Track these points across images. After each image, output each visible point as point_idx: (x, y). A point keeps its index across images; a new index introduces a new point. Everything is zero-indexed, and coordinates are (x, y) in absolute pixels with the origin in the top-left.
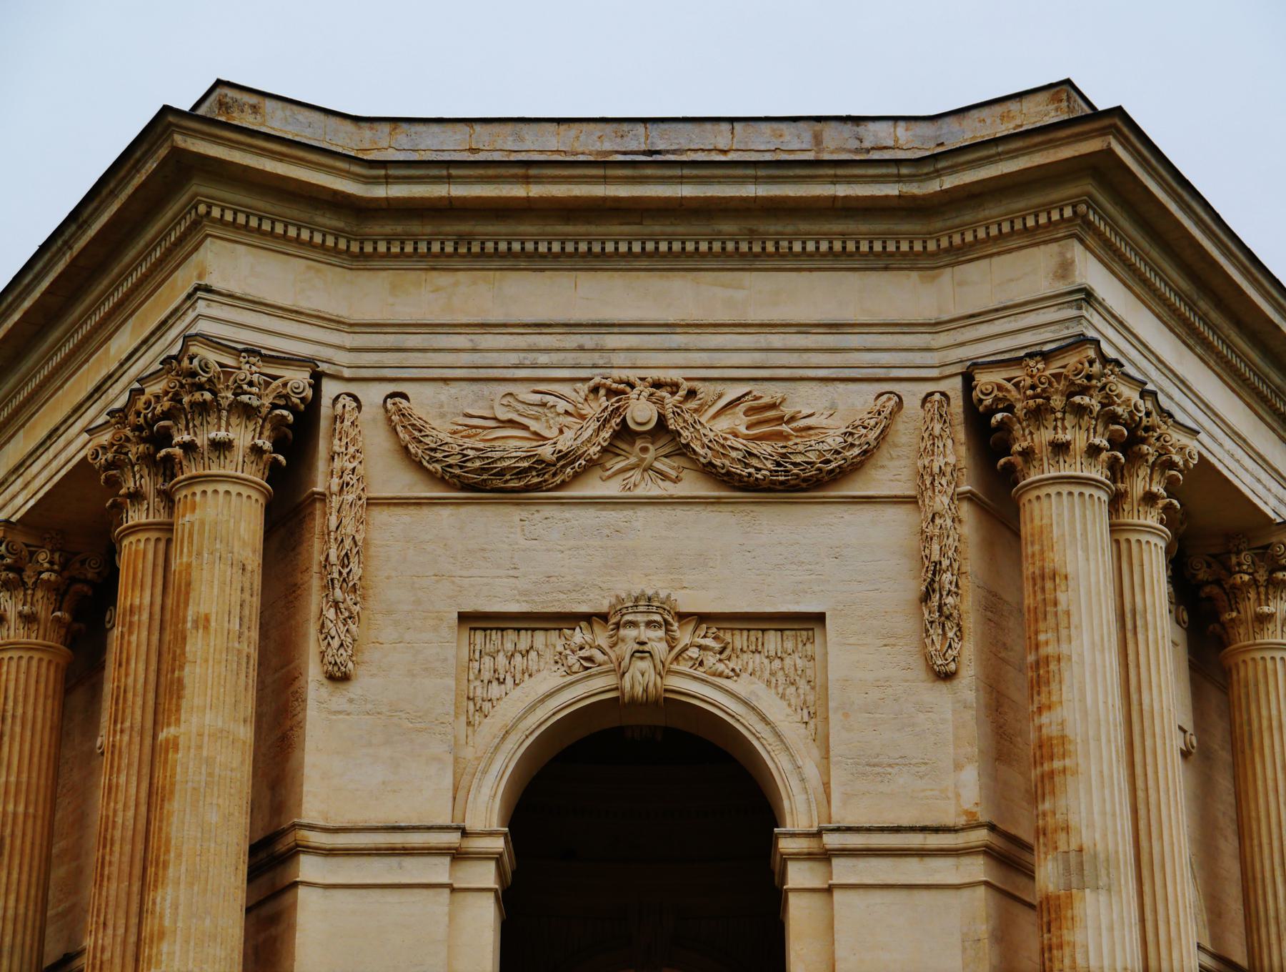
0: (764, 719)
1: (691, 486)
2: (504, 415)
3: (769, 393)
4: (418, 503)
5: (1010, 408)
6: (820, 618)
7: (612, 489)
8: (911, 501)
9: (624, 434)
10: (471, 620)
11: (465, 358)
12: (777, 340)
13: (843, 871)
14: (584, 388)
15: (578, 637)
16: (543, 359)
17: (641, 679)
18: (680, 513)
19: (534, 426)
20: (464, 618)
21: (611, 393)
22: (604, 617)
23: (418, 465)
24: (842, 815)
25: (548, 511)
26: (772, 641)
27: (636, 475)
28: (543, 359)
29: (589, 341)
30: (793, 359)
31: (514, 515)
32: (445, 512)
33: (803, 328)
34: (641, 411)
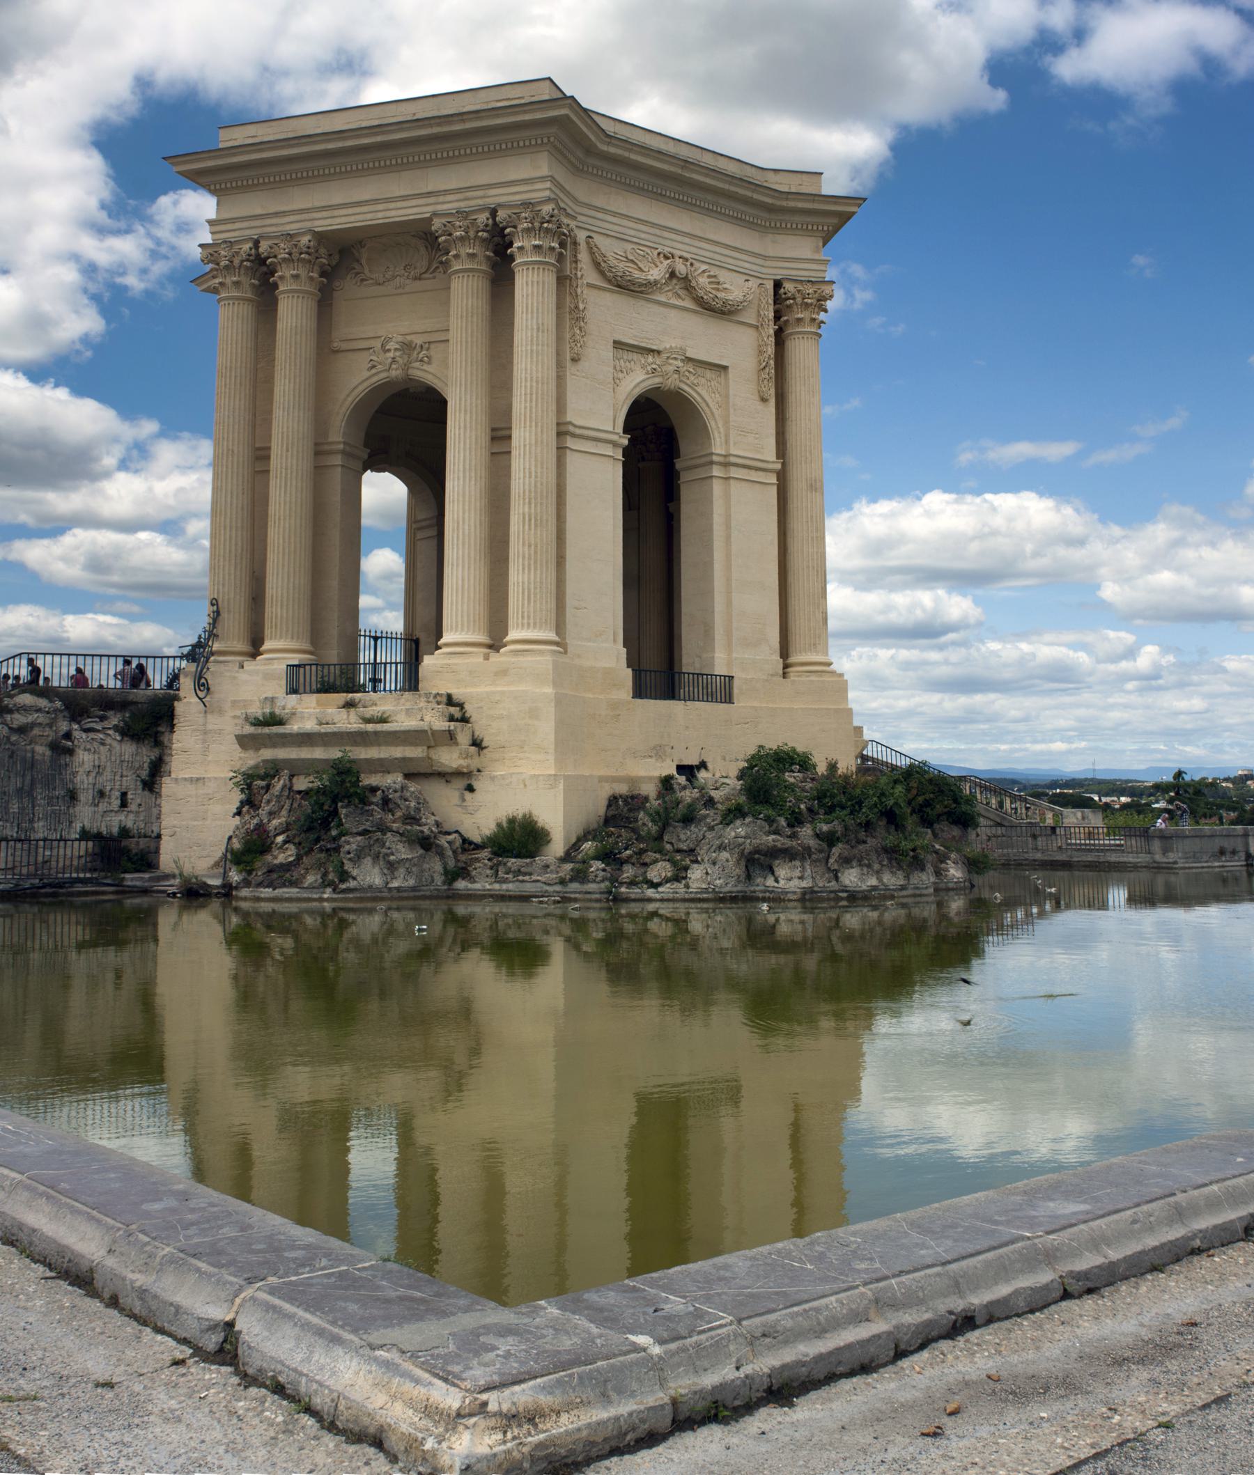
0: (708, 405)
1: (688, 304)
2: (631, 257)
3: (714, 271)
4: (605, 289)
5: (794, 299)
6: (725, 368)
7: (662, 298)
8: (757, 327)
9: (673, 275)
10: (618, 345)
11: (616, 228)
12: (718, 249)
13: (734, 472)
14: (656, 252)
15: (650, 359)
16: (643, 236)
17: (672, 382)
18: (685, 314)
19: (641, 265)
20: (615, 342)
21: (666, 258)
22: (659, 352)
23: (602, 273)
24: (733, 452)
25: (643, 302)
26: (708, 374)
27: (670, 294)
28: (643, 236)
29: (658, 232)
30: (722, 259)
31: (632, 301)
32: (608, 294)
33: (727, 247)
34: (681, 268)
